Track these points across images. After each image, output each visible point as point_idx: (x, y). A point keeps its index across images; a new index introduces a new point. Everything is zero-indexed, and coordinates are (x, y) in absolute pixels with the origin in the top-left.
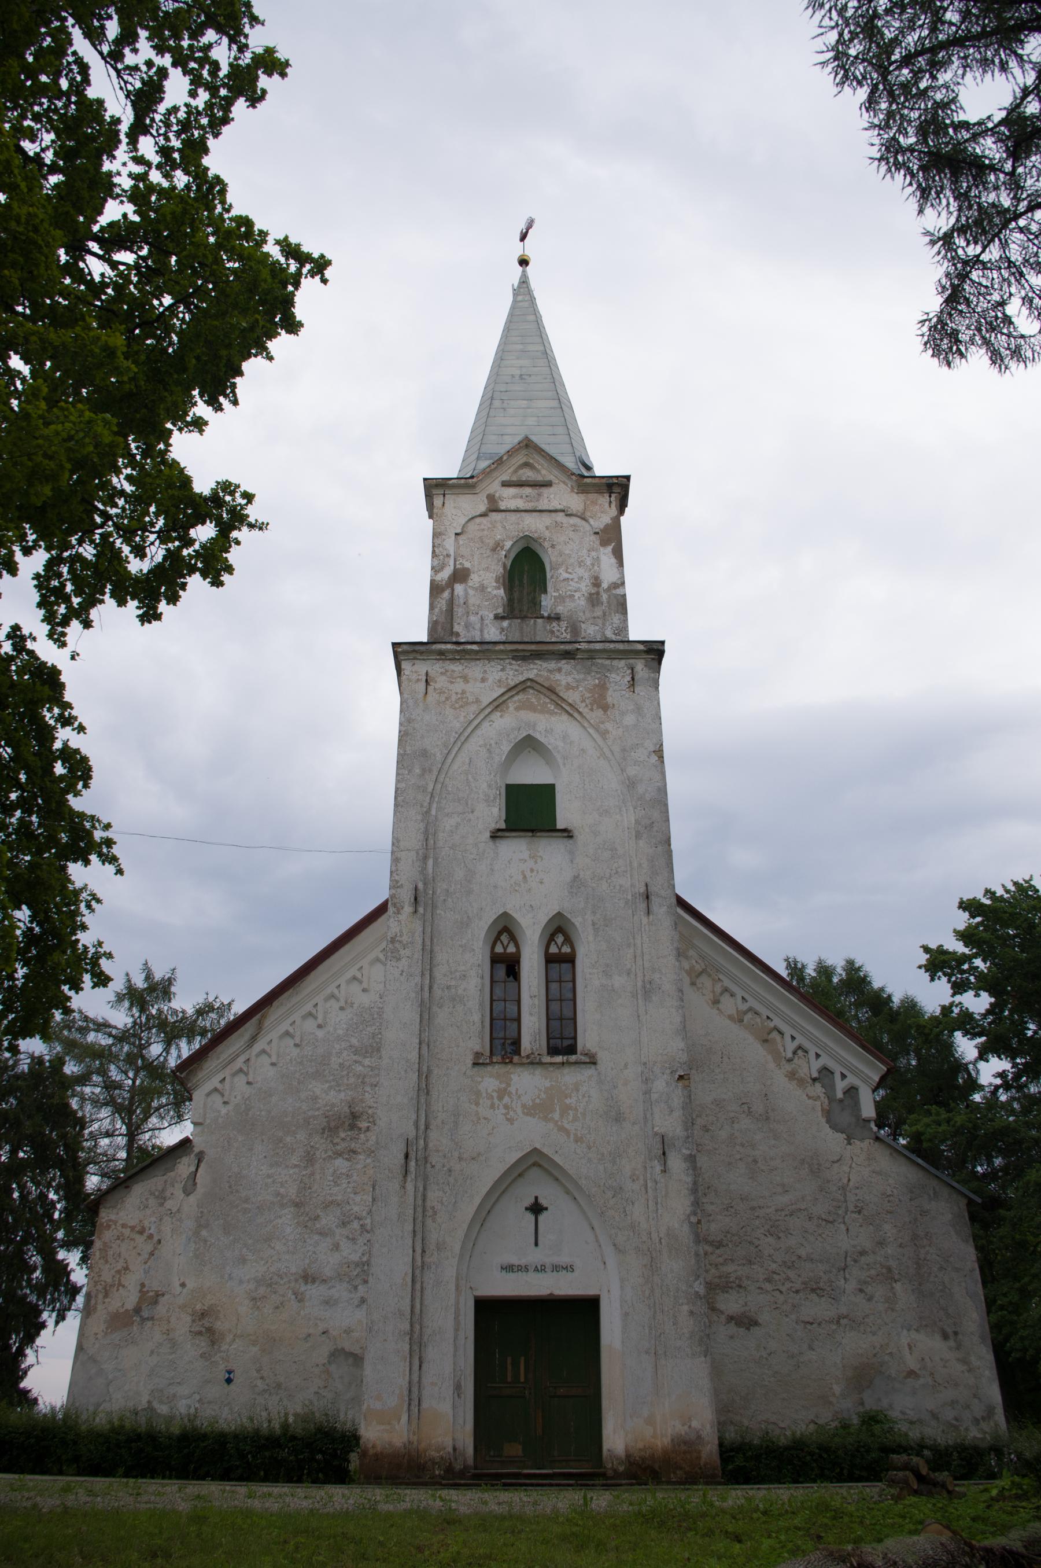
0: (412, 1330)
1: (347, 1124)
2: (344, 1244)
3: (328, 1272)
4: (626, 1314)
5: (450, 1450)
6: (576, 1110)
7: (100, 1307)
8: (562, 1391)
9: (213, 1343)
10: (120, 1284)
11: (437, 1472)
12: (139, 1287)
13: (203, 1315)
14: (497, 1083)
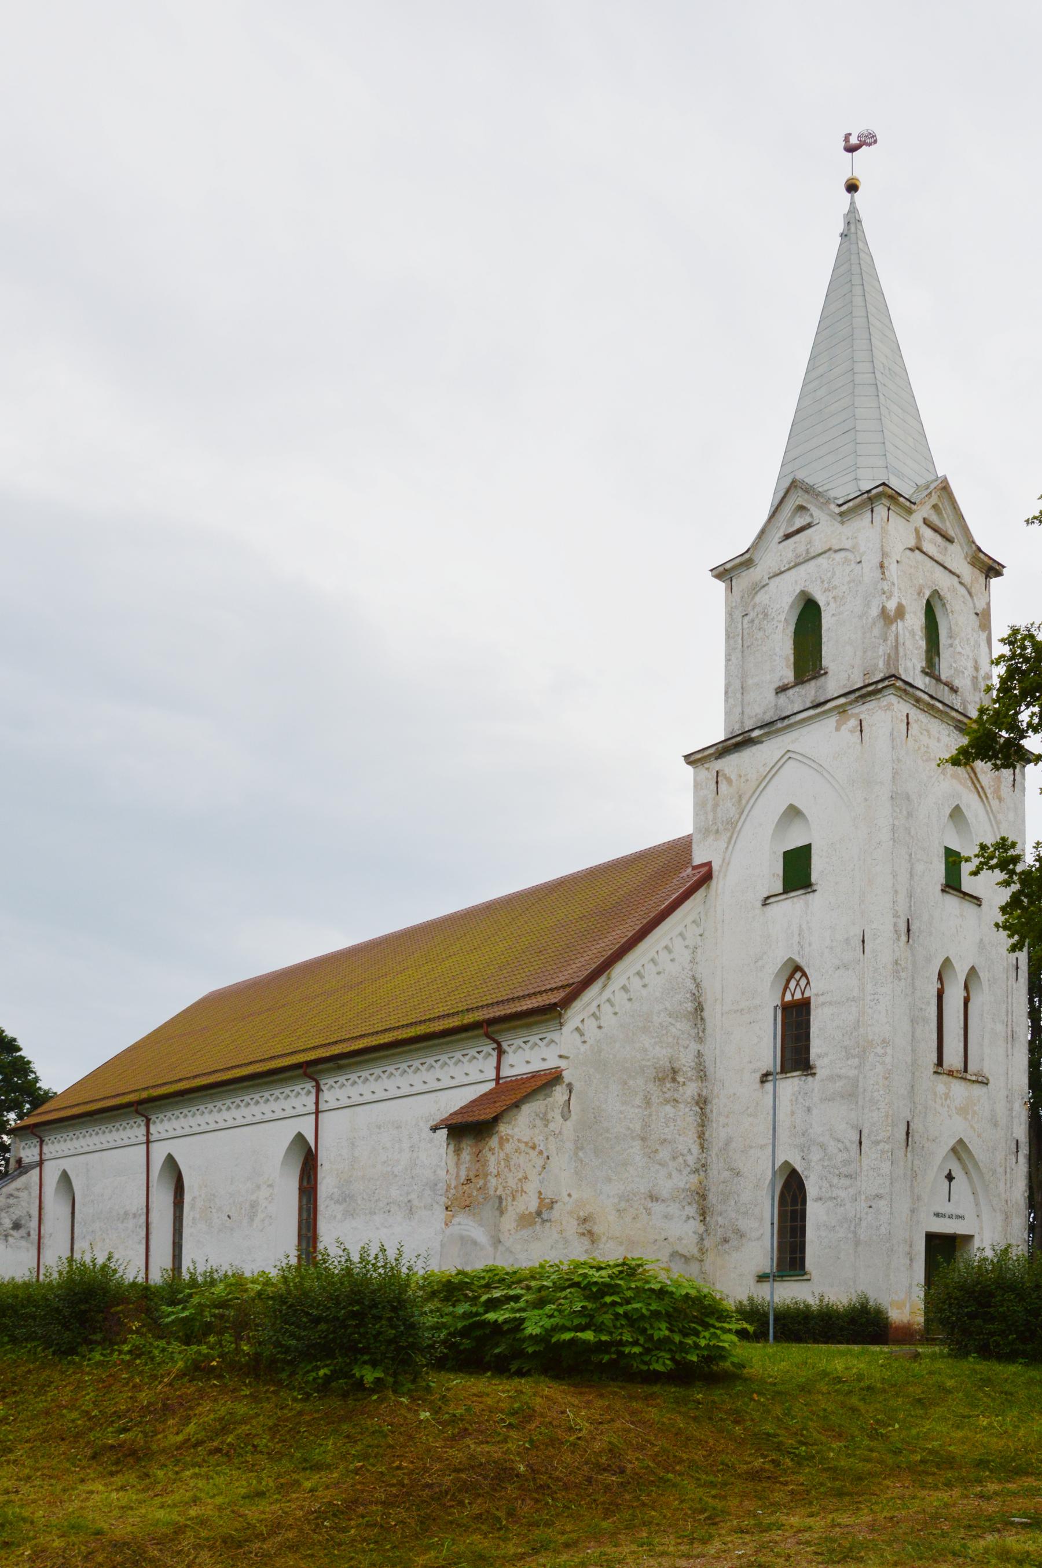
1: (670, 1076)
2: (675, 1174)
3: (665, 1194)
7: (510, 1208)
9: (593, 1242)
10: (522, 1191)
12: (537, 1195)
13: (585, 1220)
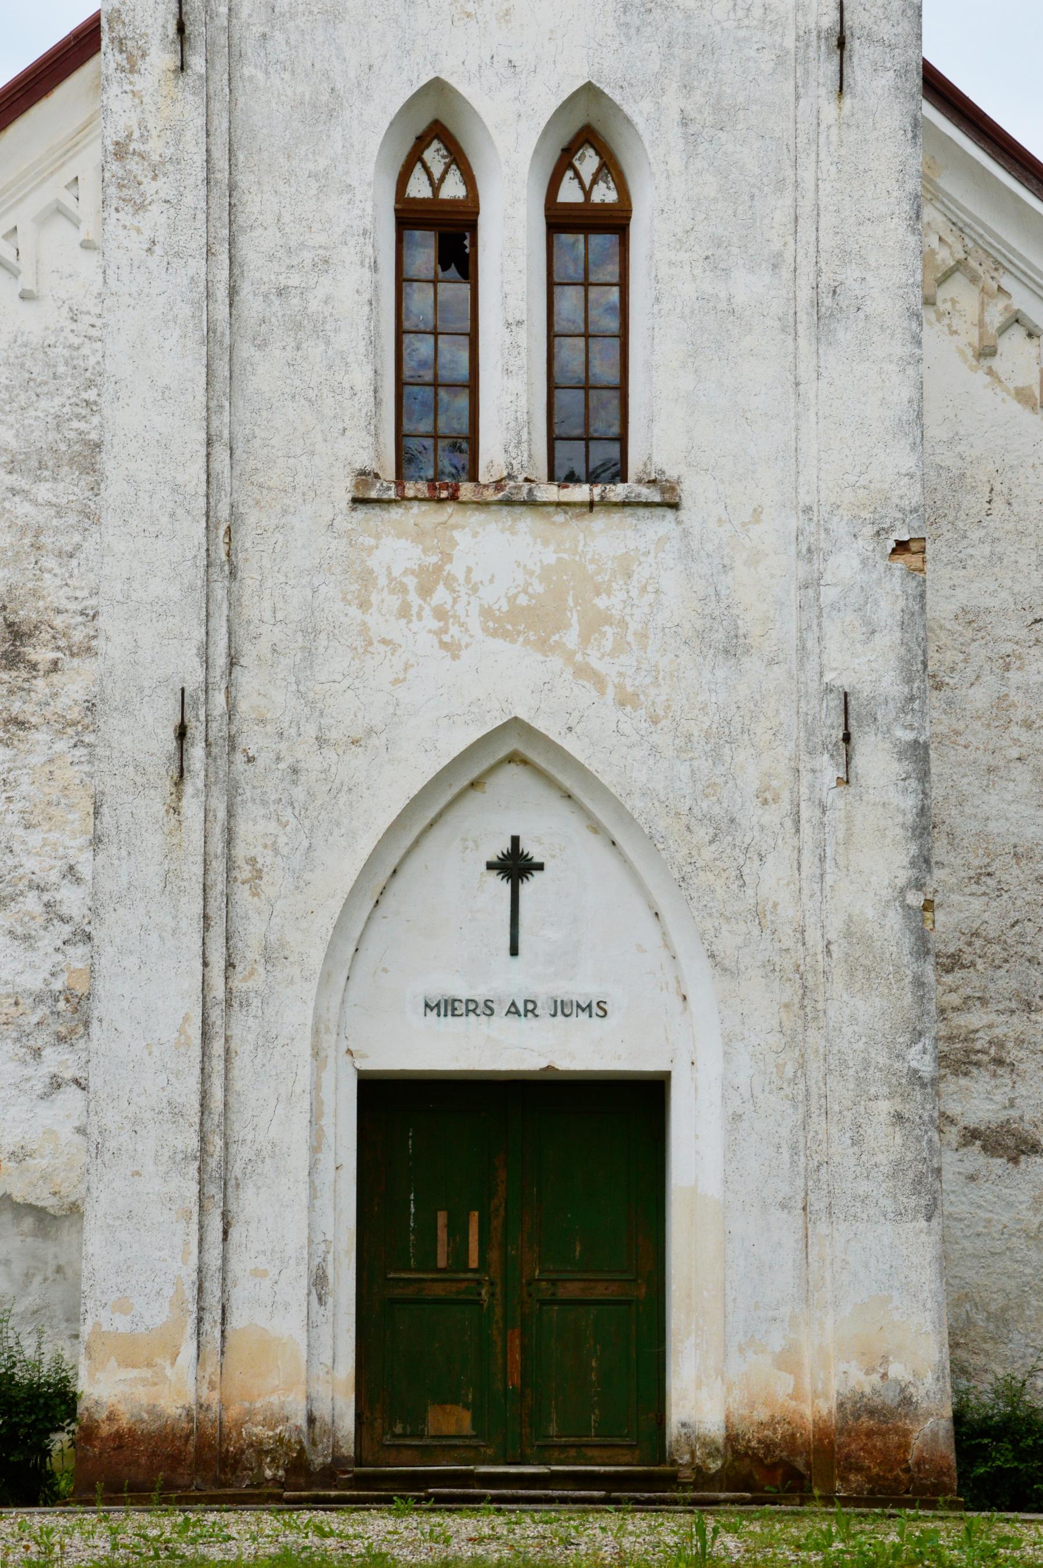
0: (203, 1150)
4: (737, 1117)
5: (301, 1421)
6: (623, 623)
8: (572, 1290)
11: (269, 1473)
14: (416, 551)
